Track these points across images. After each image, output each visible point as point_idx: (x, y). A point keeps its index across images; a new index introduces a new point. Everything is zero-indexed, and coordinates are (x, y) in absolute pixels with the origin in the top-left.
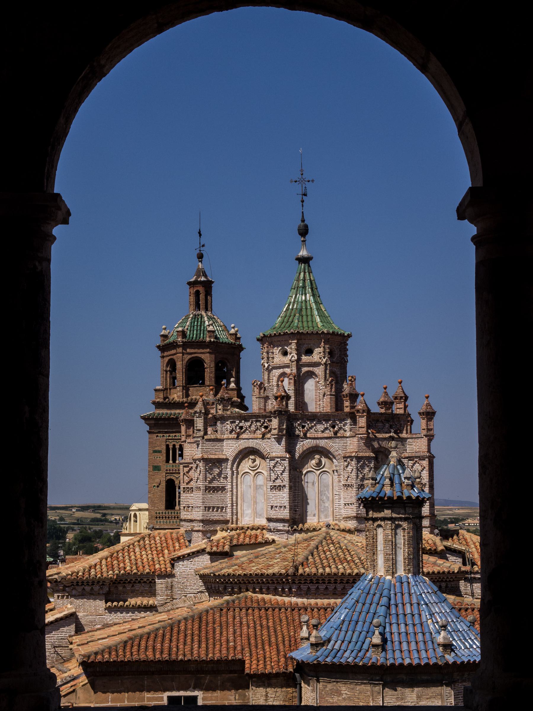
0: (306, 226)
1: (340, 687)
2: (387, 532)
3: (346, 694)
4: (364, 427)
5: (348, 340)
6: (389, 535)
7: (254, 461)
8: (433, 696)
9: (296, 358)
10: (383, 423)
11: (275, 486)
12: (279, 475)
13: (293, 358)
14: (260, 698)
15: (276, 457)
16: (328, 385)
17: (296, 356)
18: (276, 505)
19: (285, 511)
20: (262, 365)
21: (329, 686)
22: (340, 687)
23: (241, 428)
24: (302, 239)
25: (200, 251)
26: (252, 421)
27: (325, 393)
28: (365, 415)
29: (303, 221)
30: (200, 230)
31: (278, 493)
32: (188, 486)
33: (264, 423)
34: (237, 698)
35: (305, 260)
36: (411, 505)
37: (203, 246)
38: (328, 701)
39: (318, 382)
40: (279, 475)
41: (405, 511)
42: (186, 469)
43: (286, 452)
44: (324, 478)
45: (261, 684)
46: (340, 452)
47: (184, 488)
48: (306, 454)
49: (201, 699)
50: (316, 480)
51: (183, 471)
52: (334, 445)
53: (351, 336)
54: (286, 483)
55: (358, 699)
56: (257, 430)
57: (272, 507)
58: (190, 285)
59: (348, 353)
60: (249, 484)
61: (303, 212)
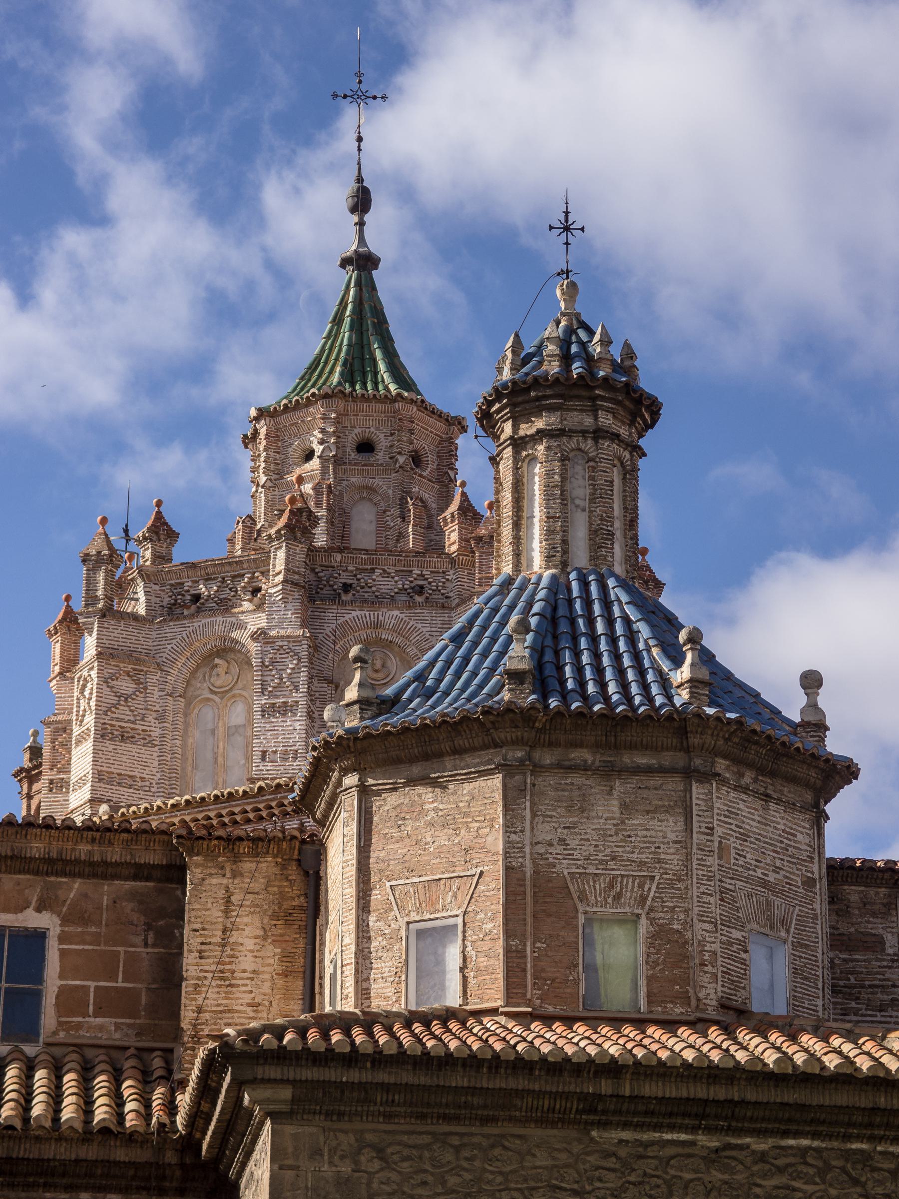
3: (436, 810)
5: (457, 438)
8: (664, 806)
14: (210, 905)
15: (278, 637)
17: (333, 448)
20: (252, 497)
22: (420, 796)
26: (223, 579)
29: (360, 180)
30: (127, 526)
31: (277, 720)
34: (150, 941)
36: (611, 405)
38: (388, 836)
39: (385, 512)
41: (596, 418)
43: (303, 625)
45: (213, 871)
49: (56, 939)
52: (420, 626)
53: (466, 431)
54: (300, 697)
57: (264, 753)
59: (458, 465)
61: (359, 163)
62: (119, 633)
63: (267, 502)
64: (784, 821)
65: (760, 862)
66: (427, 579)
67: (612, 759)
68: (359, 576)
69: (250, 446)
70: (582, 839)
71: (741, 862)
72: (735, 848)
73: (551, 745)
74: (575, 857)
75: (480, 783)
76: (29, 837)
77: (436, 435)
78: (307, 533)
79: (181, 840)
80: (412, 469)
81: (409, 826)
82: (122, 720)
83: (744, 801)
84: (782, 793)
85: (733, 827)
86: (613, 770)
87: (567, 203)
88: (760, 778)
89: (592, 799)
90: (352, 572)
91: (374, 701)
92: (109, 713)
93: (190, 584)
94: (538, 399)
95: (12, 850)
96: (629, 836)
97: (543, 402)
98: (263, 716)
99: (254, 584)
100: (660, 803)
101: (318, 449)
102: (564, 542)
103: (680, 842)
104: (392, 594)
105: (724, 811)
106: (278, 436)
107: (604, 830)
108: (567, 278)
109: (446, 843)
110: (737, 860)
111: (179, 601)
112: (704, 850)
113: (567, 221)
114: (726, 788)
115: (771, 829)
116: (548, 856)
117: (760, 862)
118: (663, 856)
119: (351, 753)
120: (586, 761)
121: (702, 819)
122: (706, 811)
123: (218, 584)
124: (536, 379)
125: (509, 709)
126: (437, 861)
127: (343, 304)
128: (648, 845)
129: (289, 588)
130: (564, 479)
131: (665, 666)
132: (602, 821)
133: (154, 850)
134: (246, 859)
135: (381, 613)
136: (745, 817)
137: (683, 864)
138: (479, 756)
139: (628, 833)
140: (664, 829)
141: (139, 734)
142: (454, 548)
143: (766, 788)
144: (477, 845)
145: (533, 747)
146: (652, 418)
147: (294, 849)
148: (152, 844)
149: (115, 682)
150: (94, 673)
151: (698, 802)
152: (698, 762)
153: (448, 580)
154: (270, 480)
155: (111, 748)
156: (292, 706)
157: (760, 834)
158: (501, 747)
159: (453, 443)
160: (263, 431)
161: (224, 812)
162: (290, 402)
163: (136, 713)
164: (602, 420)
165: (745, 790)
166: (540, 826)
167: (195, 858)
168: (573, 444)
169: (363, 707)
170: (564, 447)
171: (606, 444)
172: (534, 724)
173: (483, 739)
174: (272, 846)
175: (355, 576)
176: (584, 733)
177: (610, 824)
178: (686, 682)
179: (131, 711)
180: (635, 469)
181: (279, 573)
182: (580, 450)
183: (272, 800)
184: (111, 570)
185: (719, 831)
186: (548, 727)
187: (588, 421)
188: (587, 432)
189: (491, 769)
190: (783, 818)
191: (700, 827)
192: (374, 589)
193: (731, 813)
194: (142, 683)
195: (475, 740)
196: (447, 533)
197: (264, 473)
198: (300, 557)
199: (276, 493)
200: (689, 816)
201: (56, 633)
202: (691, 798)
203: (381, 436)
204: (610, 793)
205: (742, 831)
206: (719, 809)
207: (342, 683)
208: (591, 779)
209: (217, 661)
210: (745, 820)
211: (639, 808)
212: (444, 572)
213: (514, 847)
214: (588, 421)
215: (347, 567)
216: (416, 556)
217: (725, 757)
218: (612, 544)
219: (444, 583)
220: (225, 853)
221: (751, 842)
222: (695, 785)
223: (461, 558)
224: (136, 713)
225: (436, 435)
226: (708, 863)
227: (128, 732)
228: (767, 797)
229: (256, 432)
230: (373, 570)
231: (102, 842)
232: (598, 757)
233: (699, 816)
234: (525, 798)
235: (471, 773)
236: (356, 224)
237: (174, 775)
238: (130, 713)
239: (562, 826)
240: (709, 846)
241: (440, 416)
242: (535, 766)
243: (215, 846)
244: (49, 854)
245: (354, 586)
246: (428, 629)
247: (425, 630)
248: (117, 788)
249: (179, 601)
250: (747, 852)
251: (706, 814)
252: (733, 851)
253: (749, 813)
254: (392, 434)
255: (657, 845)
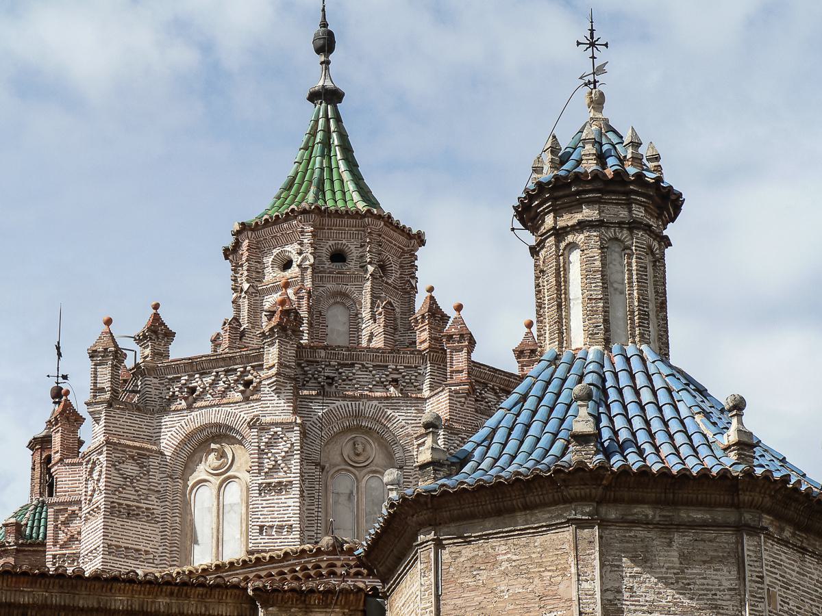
0: (330, 35)
1: (493, 548)
2: (590, 253)
3: (509, 560)
4: (461, 372)
6: (595, 260)
7: (222, 455)
8: (719, 557)
9: (312, 261)
10: (496, 393)
11: (270, 484)
12: (279, 462)
13: (308, 263)
15: (273, 424)
16: (380, 314)
18: (271, 524)
19: (291, 536)
21: (467, 551)
22: (493, 548)
23: (193, 390)
24: (322, 58)
25: (57, 383)
26: (217, 372)
27: (372, 333)
28: (466, 346)
30: (59, 343)
31: (273, 498)
32: (64, 552)
33: (245, 372)
35: (331, 96)
37: (65, 377)
38: (465, 585)
40: (279, 462)
41: (630, 211)
42: (62, 518)
43: (295, 412)
44: (373, 485)
46: (410, 430)
47: (54, 557)
48: (337, 434)
50: (355, 492)
51: (56, 520)
55: (541, 566)
56: (228, 388)
57: (261, 528)
58: (32, 450)
59: (417, 274)
60: (207, 504)
61: (323, 10)
62: (125, 420)
63: (250, 305)
64: (818, 572)
65: (801, 609)
66: (401, 373)
67: (671, 514)
68: (340, 370)
69: (231, 257)
70: (646, 587)
71: (786, 609)
72: (780, 595)
73: (616, 501)
74: (641, 603)
75: (551, 536)
76: (113, 591)
77: (399, 247)
78: (297, 333)
79: (258, 592)
80: (381, 277)
81: (484, 576)
82: (128, 499)
83: (786, 553)
84: (814, 545)
85: (778, 576)
86: (672, 524)
87: (592, 22)
88: (797, 532)
89: (653, 549)
90: (334, 366)
91: (445, 462)
92: (117, 493)
93: (186, 378)
94: (578, 193)
95: (99, 603)
96: (689, 584)
97: (583, 196)
98: (260, 494)
99: (246, 378)
100: (715, 554)
101: (297, 259)
102: (606, 321)
103: (735, 589)
104: (371, 386)
105: (770, 561)
106: (258, 248)
107: (665, 578)
108: (595, 87)
109: (520, 591)
110: (782, 606)
111: (177, 393)
112: (756, 597)
113: (592, 38)
114: (770, 541)
115: (807, 579)
116: (617, 602)
117: (801, 609)
118: (719, 602)
119: (428, 509)
120: (647, 516)
121: (753, 569)
122: (756, 561)
123: (213, 378)
124: (577, 175)
125: (581, 467)
126: (512, 607)
127: (313, 134)
128: (706, 592)
129: (282, 380)
130: (604, 265)
131: (709, 432)
132: (664, 570)
133: (227, 603)
134: (317, 610)
135: (361, 403)
136: (787, 568)
137: (738, 610)
138: (549, 512)
139: (687, 581)
140: (719, 578)
141: (143, 512)
142: (426, 345)
143: (802, 542)
144: (551, 593)
145: (599, 503)
146: (674, 213)
147: (360, 600)
148: (224, 598)
149: (122, 466)
150: (103, 458)
151: (749, 553)
152: (747, 517)
153: (420, 374)
154: (253, 286)
155: (119, 524)
156: (286, 485)
157: (799, 584)
158: (571, 503)
159: (414, 254)
160: (246, 243)
161: (251, 576)
162: (271, 218)
163: (140, 493)
164: (635, 212)
165: (785, 542)
166: (608, 575)
167: (270, 609)
168: (611, 233)
169: (436, 468)
170: (603, 236)
171: (640, 234)
172: (602, 480)
173: (553, 496)
174: (340, 598)
175: (337, 370)
176: (645, 490)
177: (670, 573)
178: (734, 445)
179: (136, 491)
180: (663, 257)
181: (274, 365)
182: (616, 239)
183: (294, 564)
184: (116, 365)
185: (767, 580)
186: (613, 484)
187: (623, 213)
188: (623, 223)
189: (562, 523)
190: (816, 569)
191: (752, 576)
192: (354, 381)
193: (776, 564)
194: (145, 466)
195: (546, 497)
196: (417, 332)
197: (247, 280)
198: (292, 352)
199: (257, 298)
200: (741, 566)
201: (56, 424)
202: (743, 549)
203: (353, 247)
204: (670, 545)
205: (785, 580)
206: (766, 559)
207: (327, 465)
208: (653, 533)
209: (213, 446)
210: (787, 570)
211: (696, 558)
212: (416, 367)
213: (586, 595)
214: (623, 213)
215: (329, 362)
216: (392, 353)
217: (768, 514)
218: (648, 324)
219: (416, 376)
220: (297, 604)
221: (793, 591)
222: (745, 536)
223: (432, 354)
224: (140, 493)
225: (399, 247)
226: (760, 609)
227: (134, 510)
228: (803, 550)
229: (237, 245)
230: (352, 365)
231: (179, 595)
232: (658, 511)
233: (751, 566)
234: (594, 548)
235: (543, 526)
236: (322, 63)
237: (175, 548)
238: (133, 492)
239: (628, 575)
240: (760, 593)
241: (403, 231)
242: (602, 520)
243: (289, 597)
244: (131, 606)
245: (336, 379)
246: (405, 418)
247: (402, 418)
248: (125, 560)
249: (177, 393)
250: (790, 599)
251: (756, 564)
252: (779, 598)
253: (790, 564)
254: (362, 246)
255: (713, 592)
